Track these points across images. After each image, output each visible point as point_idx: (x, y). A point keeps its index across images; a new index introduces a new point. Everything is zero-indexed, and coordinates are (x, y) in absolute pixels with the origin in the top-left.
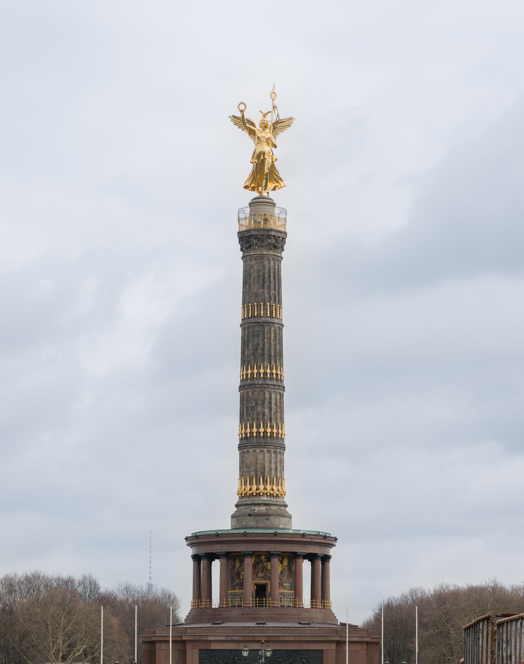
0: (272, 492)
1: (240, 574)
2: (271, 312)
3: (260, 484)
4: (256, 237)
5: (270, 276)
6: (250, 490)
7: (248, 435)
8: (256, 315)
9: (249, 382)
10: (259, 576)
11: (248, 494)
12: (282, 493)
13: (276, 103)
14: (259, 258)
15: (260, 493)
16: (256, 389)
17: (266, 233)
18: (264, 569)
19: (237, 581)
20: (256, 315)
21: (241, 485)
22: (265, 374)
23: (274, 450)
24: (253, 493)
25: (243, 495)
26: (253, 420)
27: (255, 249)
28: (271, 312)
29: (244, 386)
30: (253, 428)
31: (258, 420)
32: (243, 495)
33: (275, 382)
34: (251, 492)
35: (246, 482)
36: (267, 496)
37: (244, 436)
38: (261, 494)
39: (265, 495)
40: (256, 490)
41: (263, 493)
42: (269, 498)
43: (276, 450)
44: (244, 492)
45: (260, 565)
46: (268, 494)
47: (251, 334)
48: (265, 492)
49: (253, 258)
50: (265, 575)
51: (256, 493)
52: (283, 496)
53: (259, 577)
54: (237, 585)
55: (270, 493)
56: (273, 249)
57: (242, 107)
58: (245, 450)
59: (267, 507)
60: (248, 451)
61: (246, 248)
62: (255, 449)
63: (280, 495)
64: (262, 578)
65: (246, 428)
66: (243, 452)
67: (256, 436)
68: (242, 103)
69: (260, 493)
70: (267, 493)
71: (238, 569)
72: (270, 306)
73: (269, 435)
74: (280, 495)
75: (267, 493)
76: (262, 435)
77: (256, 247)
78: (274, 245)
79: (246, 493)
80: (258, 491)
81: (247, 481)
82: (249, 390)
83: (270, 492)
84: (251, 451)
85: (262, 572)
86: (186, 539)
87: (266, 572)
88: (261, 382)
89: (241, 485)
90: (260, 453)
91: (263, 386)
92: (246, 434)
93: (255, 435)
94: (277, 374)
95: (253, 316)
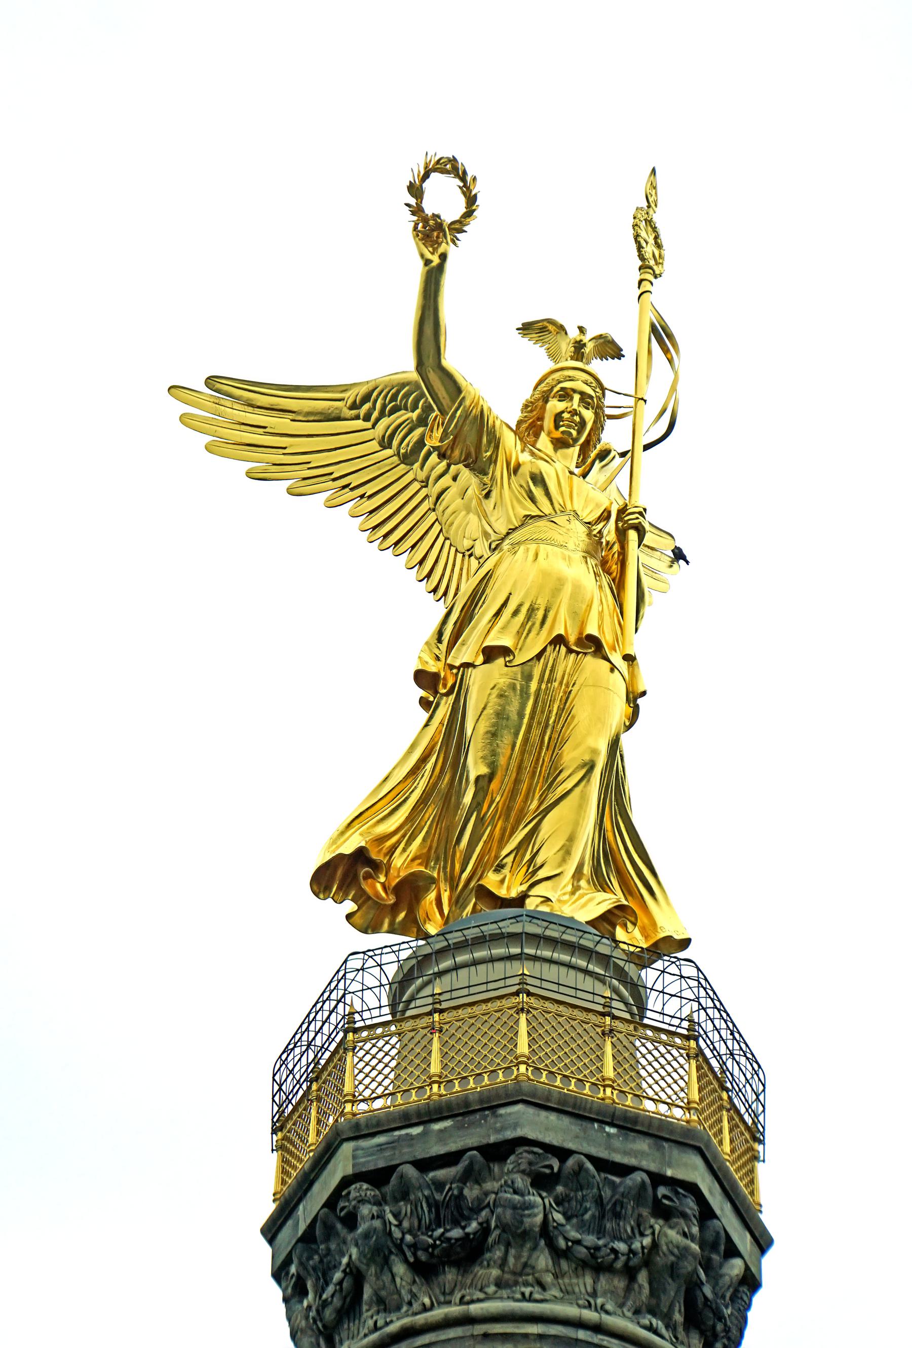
13: (666, 297)
57: (444, 198)
68: (450, 167)
77: (543, 1260)
78: (692, 1287)
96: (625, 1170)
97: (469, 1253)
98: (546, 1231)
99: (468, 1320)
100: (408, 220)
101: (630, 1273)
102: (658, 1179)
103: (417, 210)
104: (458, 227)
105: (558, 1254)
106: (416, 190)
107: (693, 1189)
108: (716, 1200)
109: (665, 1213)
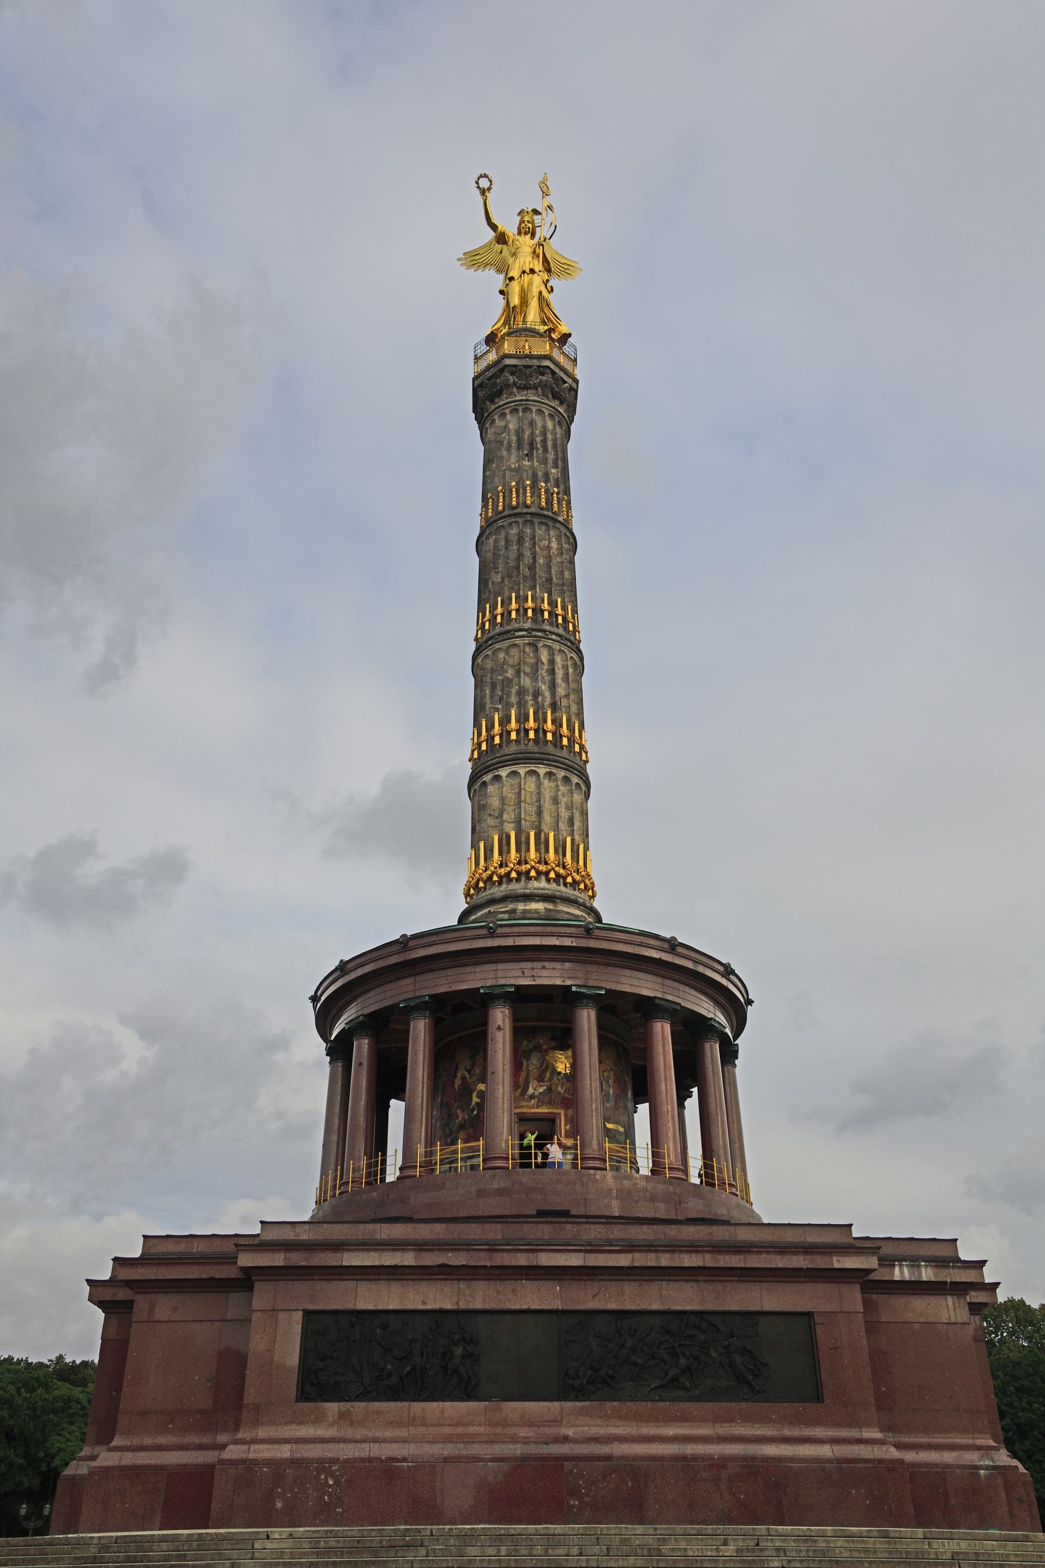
0: (562, 871)
1: (471, 1092)
2: (549, 501)
3: (528, 850)
4: (514, 370)
5: (544, 441)
6: (501, 866)
7: (497, 740)
8: (514, 503)
9: (498, 629)
10: (531, 1091)
11: (495, 878)
12: (587, 881)
14: (520, 409)
15: (528, 872)
16: (517, 641)
17: (535, 362)
18: (547, 1070)
19: (461, 1116)
20: (514, 503)
21: (477, 864)
22: (538, 611)
23: (563, 773)
24: (508, 874)
25: (481, 884)
26: (508, 706)
27: (512, 393)
28: (549, 501)
29: (486, 642)
30: (509, 722)
31: (522, 705)
32: (481, 884)
33: (561, 631)
34: (502, 871)
35: (489, 851)
36: (548, 880)
37: (484, 747)
38: (533, 873)
39: (543, 878)
40: (519, 863)
41: (539, 873)
42: (554, 886)
43: (569, 775)
44: (484, 876)
45: (535, 1061)
46: (552, 875)
47: (503, 543)
48: (542, 868)
49: (508, 411)
50: (549, 1089)
51: (518, 872)
52: (590, 893)
53: (532, 1097)
54: (462, 1127)
55: (558, 875)
56: (550, 396)
57: (484, 183)
58: (487, 778)
59: (550, 906)
60: (498, 778)
61: (492, 401)
62: (513, 768)
63: (582, 886)
64: (541, 1099)
65: (490, 727)
66: (484, 784)
67: (517, 741)
69: (528, 872)
70: (547, 873)
71: (463, 1078)
72: (547, 491)
73: (549, 736)
74: (582, 886)
75: (547, 873)
76: (532, 735)
77: (515, 390)
78: (552, 390)
79: (490, 877)
80: (524, 868)
81: (492, 850)
82: (498, 646)
83: (557, 869)
84: (504, 773)
85: (541, 1079)
86: (314, 999)
87: (551, 1079)
88: (528, 625)
89: (477, 864)
90: (529, 778)
91: (534, 633)
92: (490, 739)
93: (513, 736)
94: (564, 618)
95: (508, 505)
96: (530, 367)
97: (499, 394)
98: (514, 384)
99: (499, 407)
100: (478, 192)
101: (537, 389)
102: (539, 367)
103: (478, 187)
104: (489, 189)
105: (518, 388)
106: (477, 183)
107: (548, 367)
108: (557, 370)
109: (543, 374)
